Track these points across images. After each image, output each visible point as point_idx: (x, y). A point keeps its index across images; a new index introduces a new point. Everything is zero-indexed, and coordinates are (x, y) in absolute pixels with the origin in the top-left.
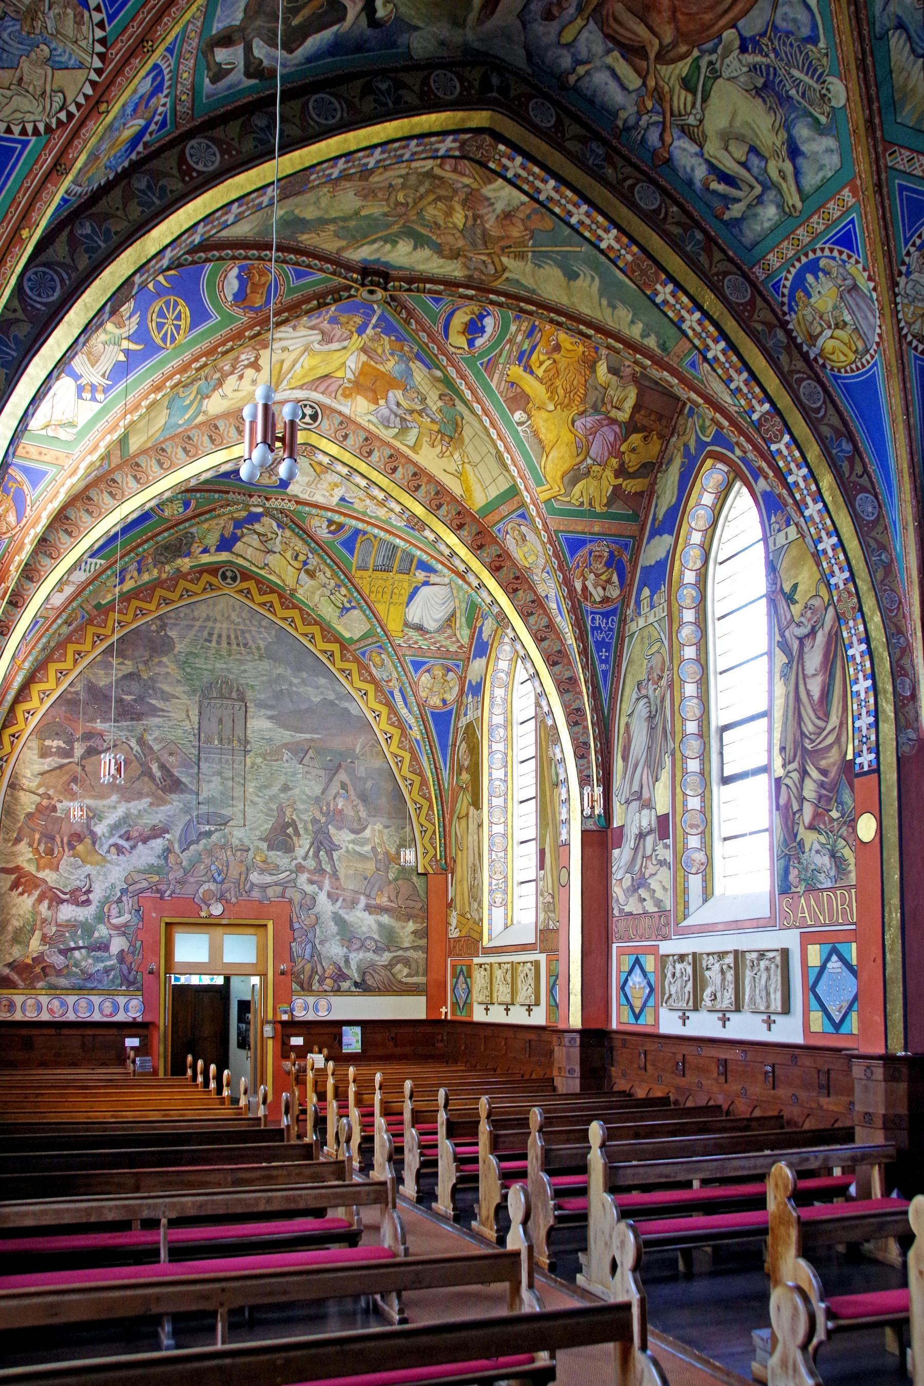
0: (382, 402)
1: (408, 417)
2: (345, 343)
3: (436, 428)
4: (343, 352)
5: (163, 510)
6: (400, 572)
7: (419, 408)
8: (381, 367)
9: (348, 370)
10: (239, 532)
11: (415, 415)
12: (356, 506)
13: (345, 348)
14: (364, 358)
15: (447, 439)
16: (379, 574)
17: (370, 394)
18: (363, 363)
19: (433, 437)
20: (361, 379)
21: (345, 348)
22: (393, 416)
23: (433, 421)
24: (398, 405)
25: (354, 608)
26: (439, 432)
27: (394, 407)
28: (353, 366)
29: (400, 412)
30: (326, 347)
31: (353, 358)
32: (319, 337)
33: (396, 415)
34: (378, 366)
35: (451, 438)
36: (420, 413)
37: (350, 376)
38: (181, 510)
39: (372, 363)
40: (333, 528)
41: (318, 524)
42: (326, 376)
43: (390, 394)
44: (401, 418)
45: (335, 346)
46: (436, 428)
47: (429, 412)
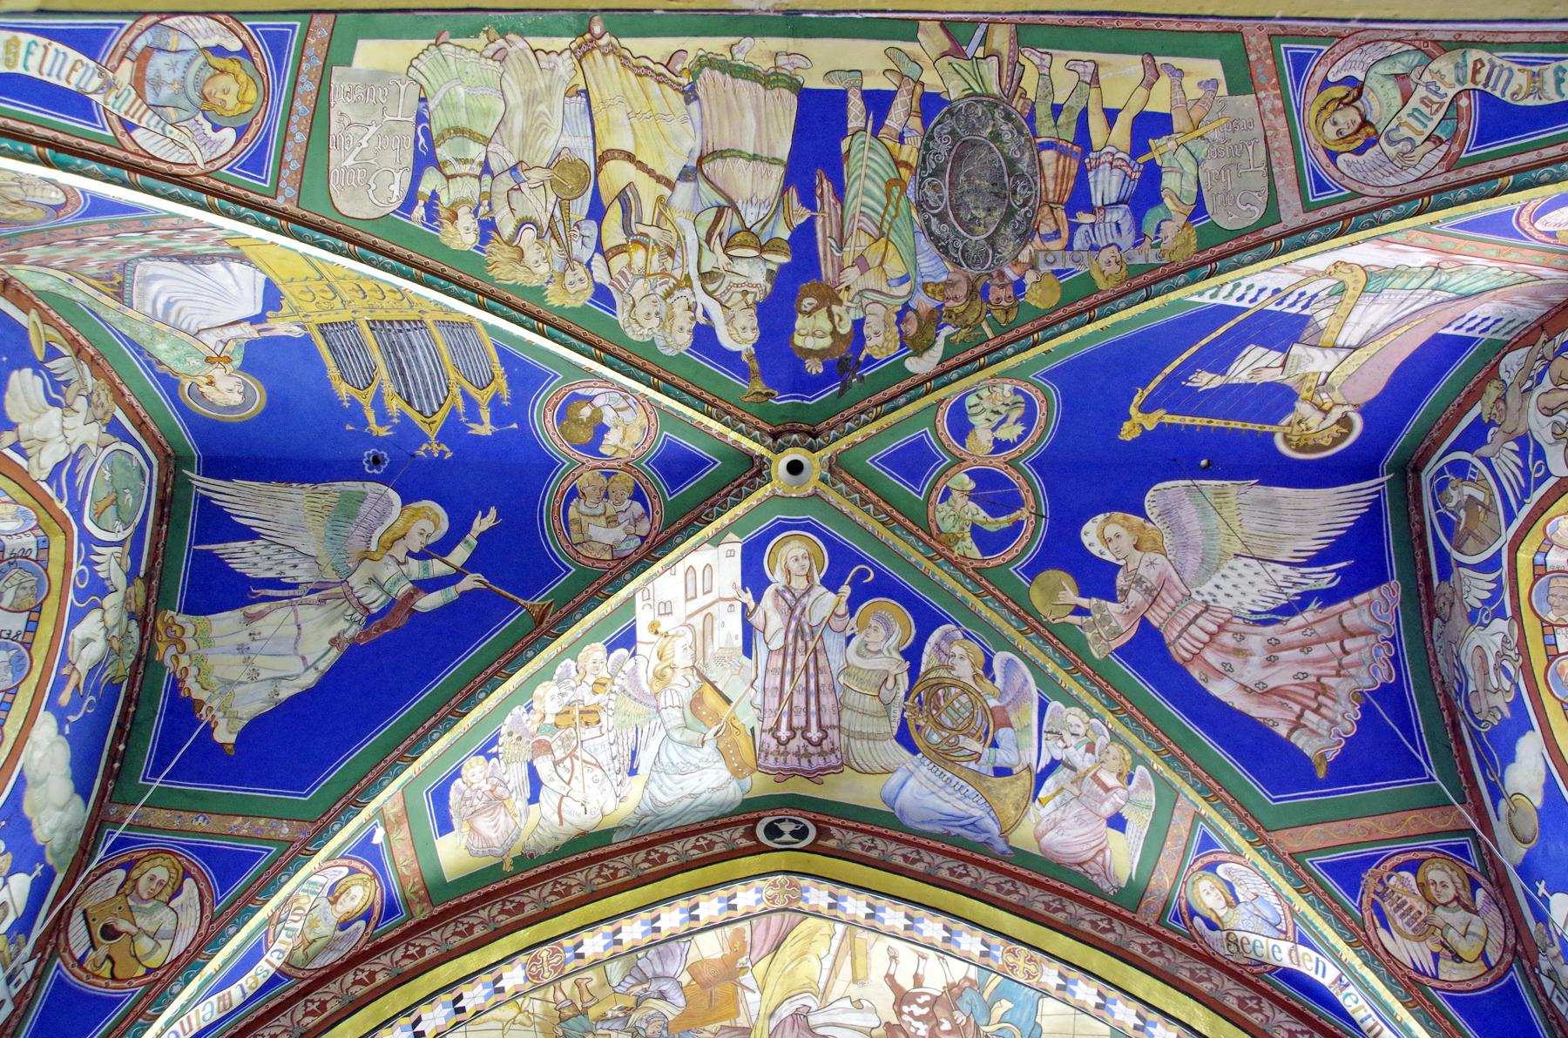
0: (685, 978)
1: (638, 989)
2: (774, 1023)
3: (593, 1012)
4: (770, 1010)
5: (1016, 391)
6: (350, 325)
7: (635, 1016)
8: (713, 1027)
9: (753, 986)
10: (801, 215)
11: (630, 1003)
12: (596, 651)
13: (772, 1015)
14: (742, 1021)
15: (567, 1012)
16: (394, 315)
17: (707, 975)
18: (738, 1014)
19: (587, 997)
20: (729, 986)
21: (772, 1015)
22: (659, 970)
23: (603, 1018)
24: (662, 996)
25: (408, 204)
26: (584, 1013)
27: (666, 986)
28: (749, 996)
29: (654, 987)
30: (797, 1004)
31: (754, 1009)
32: (813, 1020)
33: (657, 977)
34: (718, 1025)
35: (562, 1020)
36: (627, 1011)
37: (746, 979)
38: (971, 400)
39: (727, 1023)
40: (586, 412)
41: (627, 416)
42: (777, 948)
43: (681, 1002)
44: (648, 980)
45: (786, 1010)
46: (593, 1012)
47: (616, 1025)
